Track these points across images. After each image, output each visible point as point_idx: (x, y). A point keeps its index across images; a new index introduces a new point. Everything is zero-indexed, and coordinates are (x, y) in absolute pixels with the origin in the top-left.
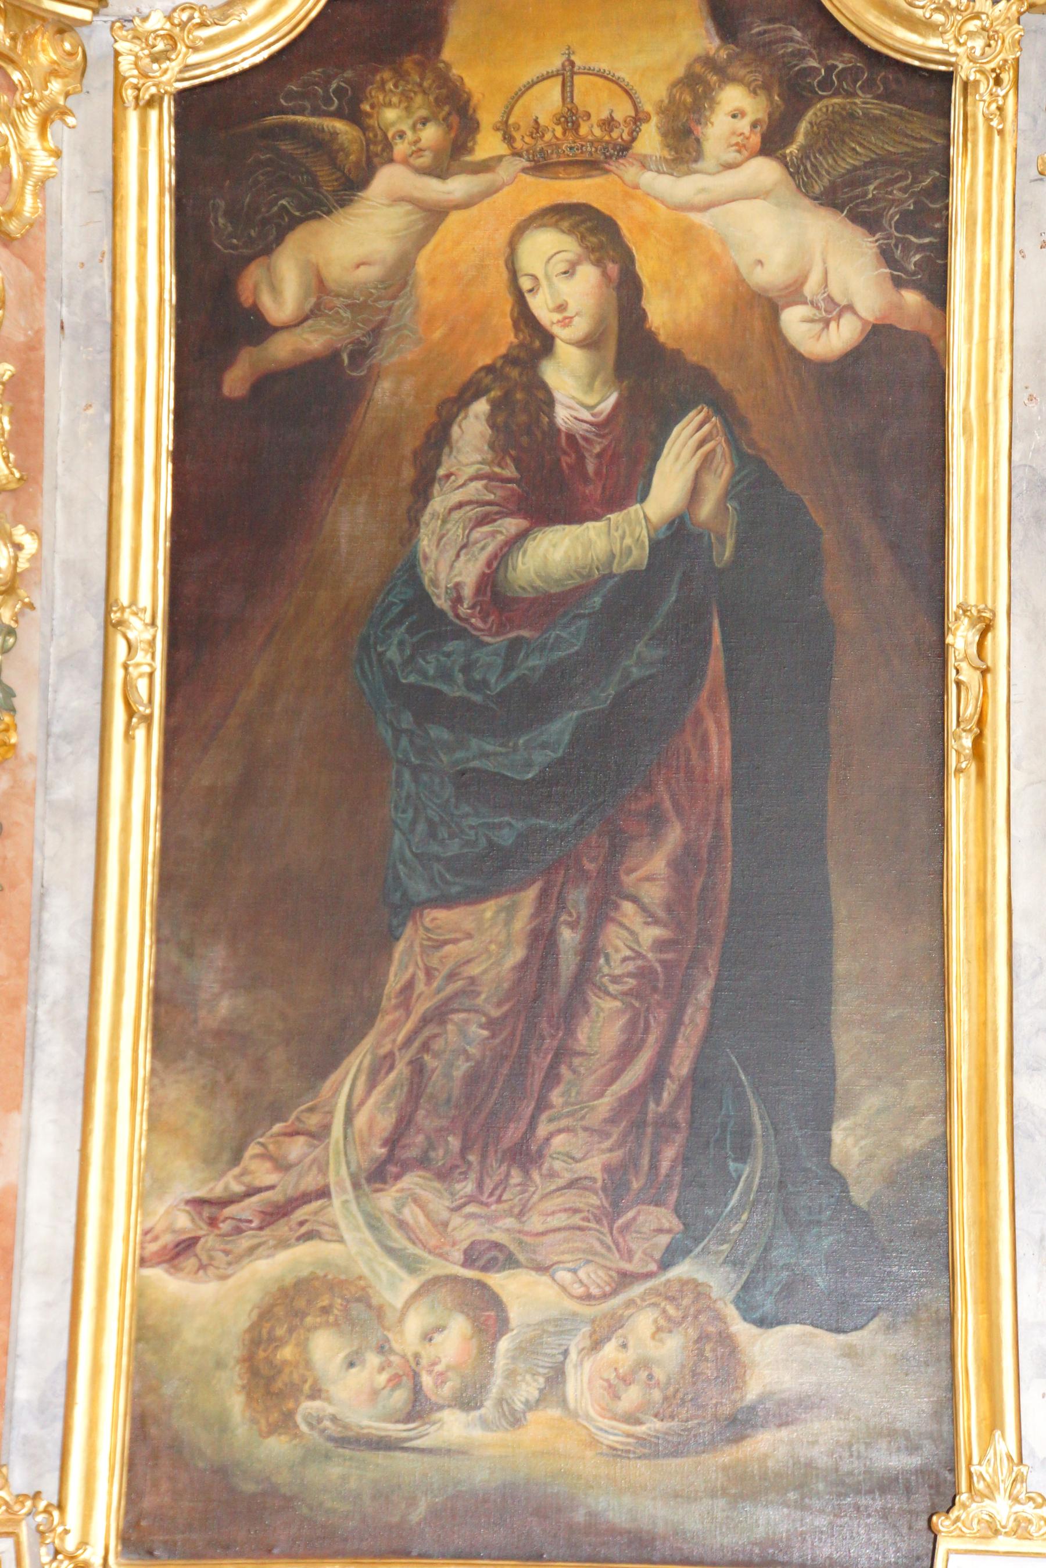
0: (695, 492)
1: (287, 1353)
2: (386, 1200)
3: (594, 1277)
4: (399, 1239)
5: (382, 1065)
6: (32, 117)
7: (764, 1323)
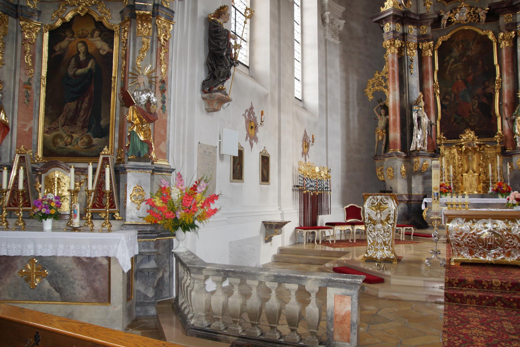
0: (92, 66)
1: (56, 141)
2: (64, 128)
3: (80, 134)
4: (65, 131)
5: (64, 116)
6: (34, 33)
7: (94, 138)
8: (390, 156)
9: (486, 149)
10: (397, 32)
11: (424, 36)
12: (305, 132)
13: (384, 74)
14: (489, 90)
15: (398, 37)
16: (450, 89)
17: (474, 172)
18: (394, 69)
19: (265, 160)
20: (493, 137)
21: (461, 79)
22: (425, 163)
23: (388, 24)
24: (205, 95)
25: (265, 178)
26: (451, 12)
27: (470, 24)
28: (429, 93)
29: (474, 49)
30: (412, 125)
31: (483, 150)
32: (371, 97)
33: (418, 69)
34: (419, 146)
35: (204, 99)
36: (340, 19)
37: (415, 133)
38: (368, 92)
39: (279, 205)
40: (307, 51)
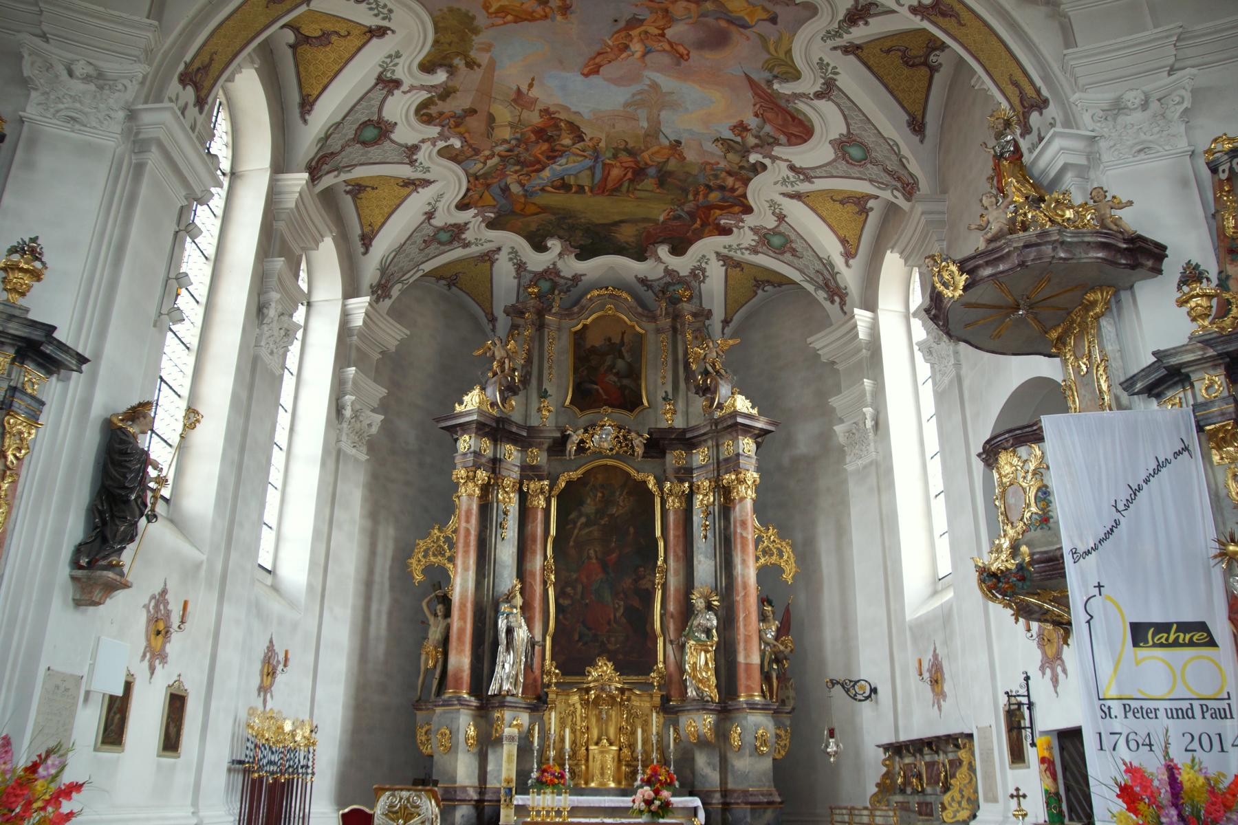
8: (447, 703)
9: (633, 697)
10: (483, 455)
11: (533, 468)
12: (271, 642)
13: (449, 533)
14: (644, 584)
15: (482, 465)
16: (574, 576)
17: (611, 744)
18: (469, 526)
19: (176, 703)
20: (648, 674)
21: (597, 558)
22: (515, 723)
23: (467, 438)
24: (79, 573)
25: (171, 743)
26: (586, 431)
27: (617, 457)
28: (535, 580)
29: (621, 504)
30: (496, 644)
31: (629, 699)
32: (419, 577)
33: (516, 530)
34: (506, 687)
35: (73, 578)
36: (374, 411)
37: (500, 659)
38: (414, 565)
39: (195, 803)
40: (295, 468)
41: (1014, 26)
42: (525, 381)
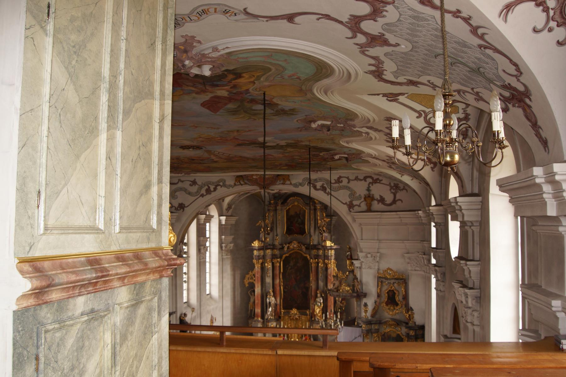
11: (275, 255)
13: (254, 273)
32: (247, 285)
41: (352, 226)
42: (272, 230)
